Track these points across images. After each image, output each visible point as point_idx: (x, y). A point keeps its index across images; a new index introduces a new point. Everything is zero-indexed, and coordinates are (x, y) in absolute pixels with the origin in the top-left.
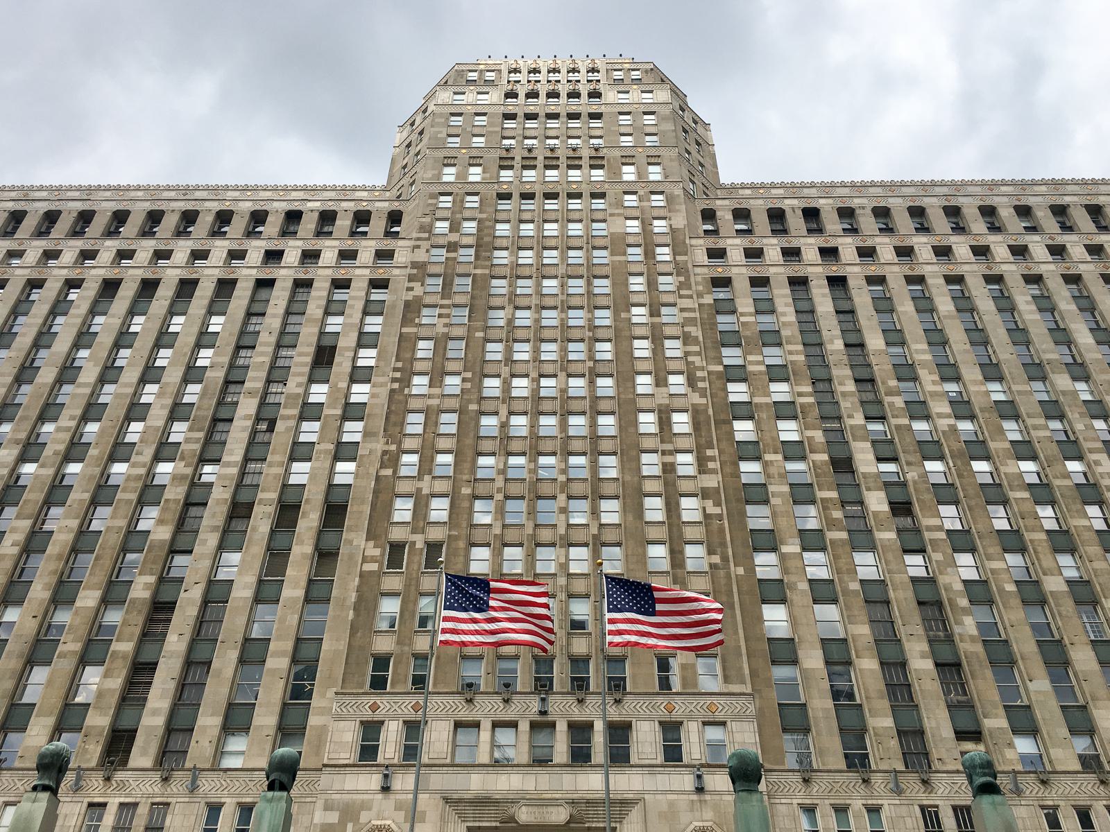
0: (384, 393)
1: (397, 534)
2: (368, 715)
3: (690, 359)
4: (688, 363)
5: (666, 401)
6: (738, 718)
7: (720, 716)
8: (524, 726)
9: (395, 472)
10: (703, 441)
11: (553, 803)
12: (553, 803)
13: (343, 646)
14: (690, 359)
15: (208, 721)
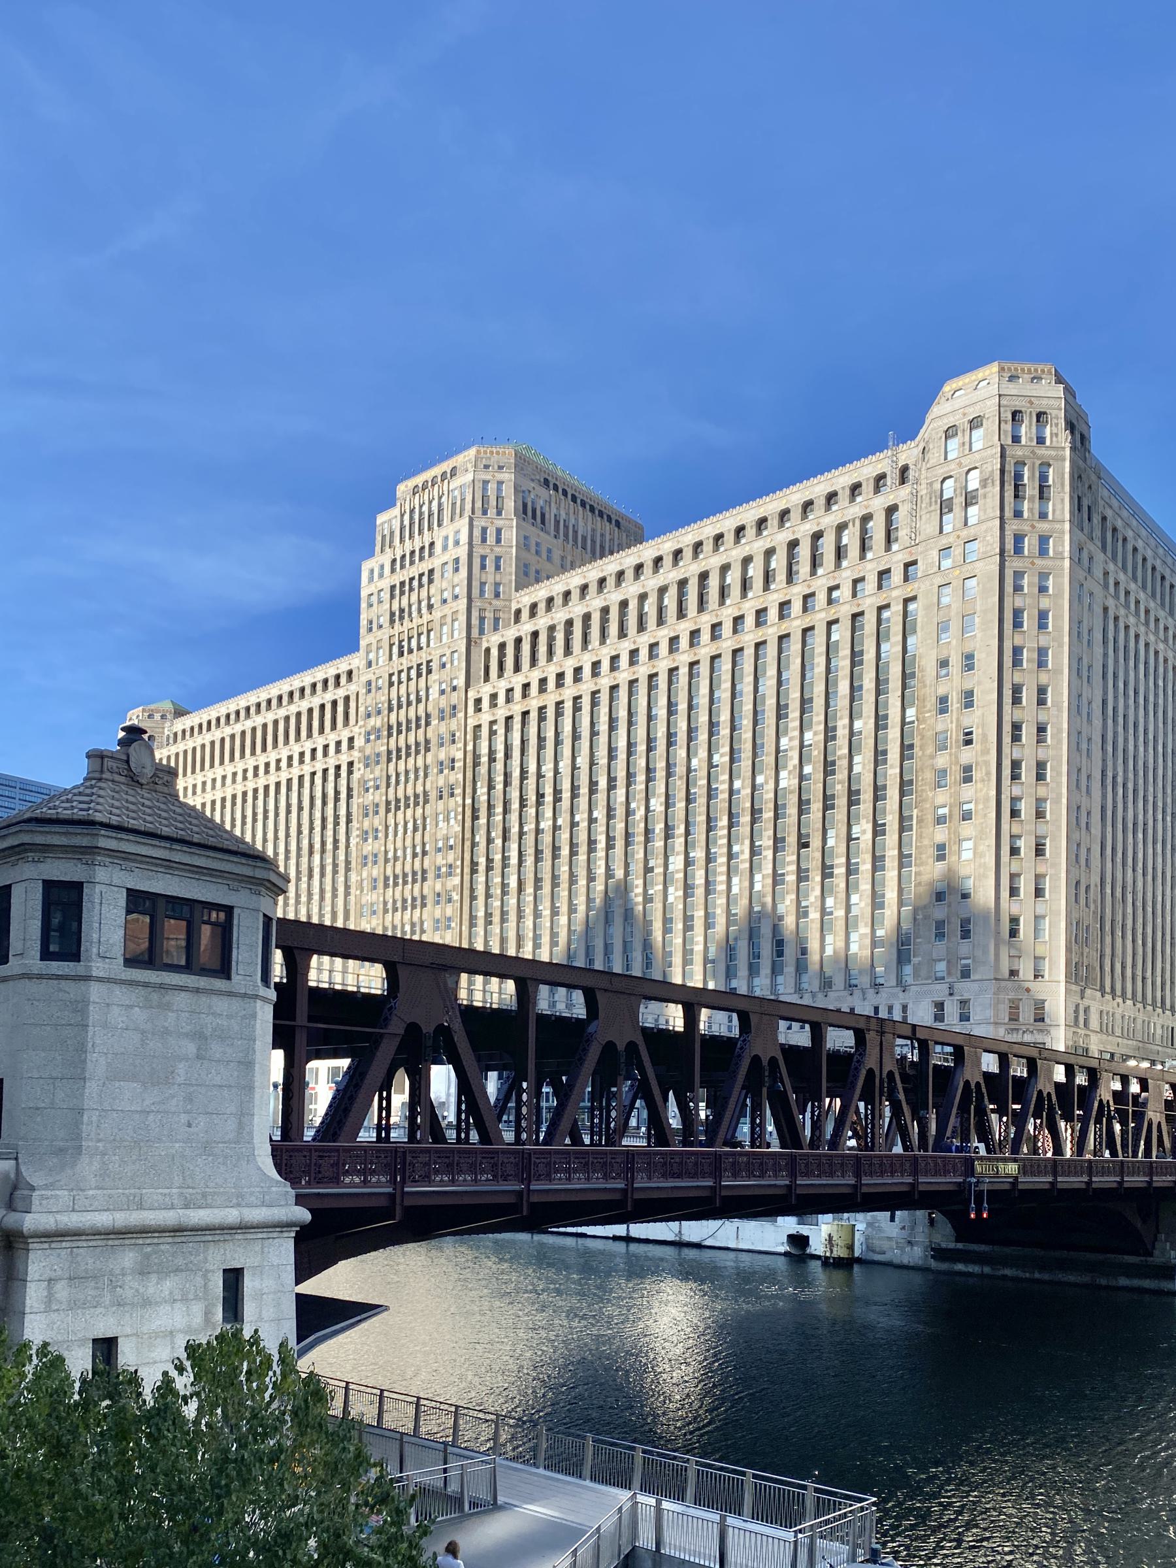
9: (362, 891)
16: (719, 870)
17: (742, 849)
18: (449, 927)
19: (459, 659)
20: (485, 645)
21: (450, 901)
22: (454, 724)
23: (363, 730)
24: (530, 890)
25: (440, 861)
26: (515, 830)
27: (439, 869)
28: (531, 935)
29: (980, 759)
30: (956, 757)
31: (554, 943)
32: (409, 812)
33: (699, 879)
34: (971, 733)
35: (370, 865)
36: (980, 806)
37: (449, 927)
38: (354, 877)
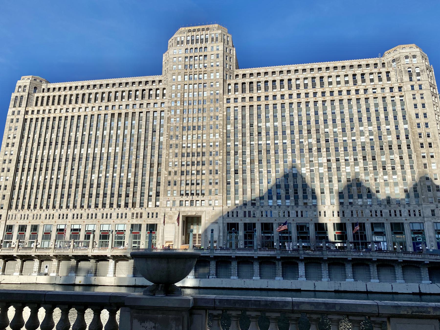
0: (165, 139)
1: (170, 169)
2: (168, 200)
3: (220, 130)
4: (220, 131)
5: (215, 140)
6: (220, 199)
7: (217, 199)
8: (190, 201)
9: (169, 157)
10: (220, 149)
11: (193, 212)
12: (193, 212)
13: (163, 189)
14: (220, 130)
15: (146, 201)
16: (341, 164)
17: (351, 159)
18: (217, 173)
19: (220, 85)
20: (228, 82)
21: (217, 164)
22: (217, 105)
23: (170, 101)
24: (256, 163)
25: (211, 149)
26: (248, 143)
27: (211, 152)
28: (258, 179)
29: (434, 142)
30: (426, 140)
31: (268, 183)
32: (195, 132)
33: (334, 166)
34: (429, 134)
35: (174, 148)
36: (437, 154)
37: (217, 173)
38: (164, 152)
